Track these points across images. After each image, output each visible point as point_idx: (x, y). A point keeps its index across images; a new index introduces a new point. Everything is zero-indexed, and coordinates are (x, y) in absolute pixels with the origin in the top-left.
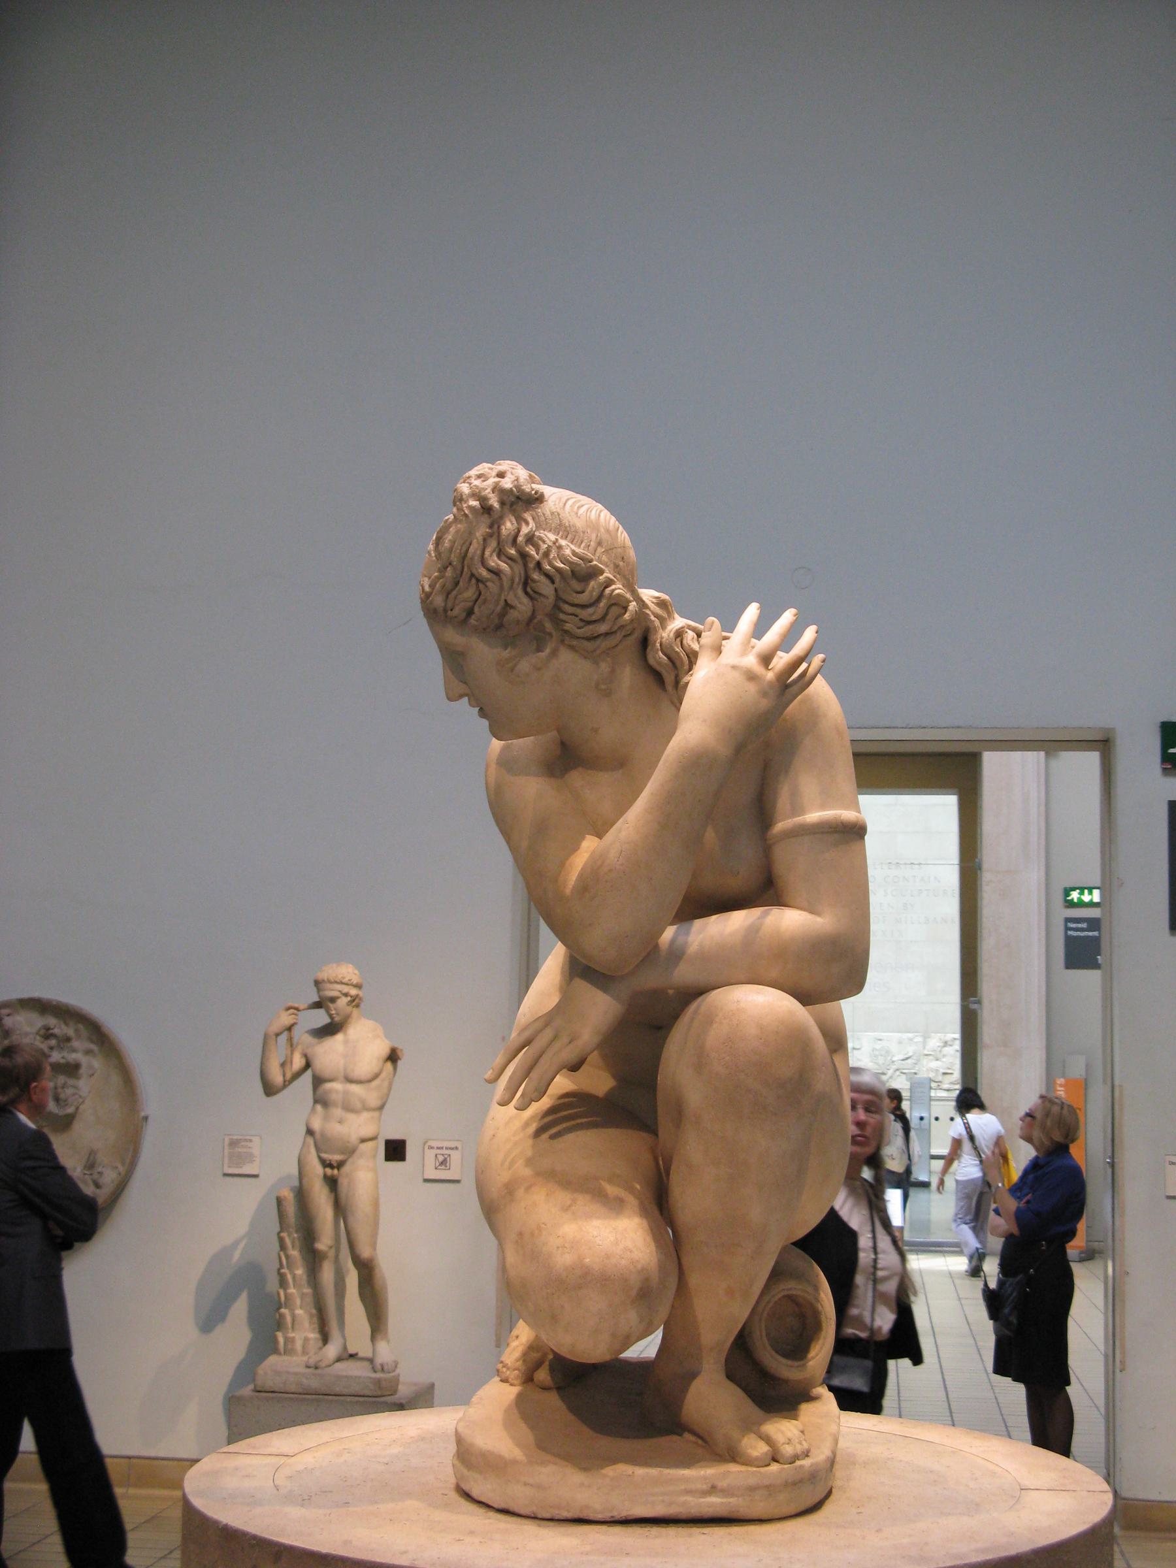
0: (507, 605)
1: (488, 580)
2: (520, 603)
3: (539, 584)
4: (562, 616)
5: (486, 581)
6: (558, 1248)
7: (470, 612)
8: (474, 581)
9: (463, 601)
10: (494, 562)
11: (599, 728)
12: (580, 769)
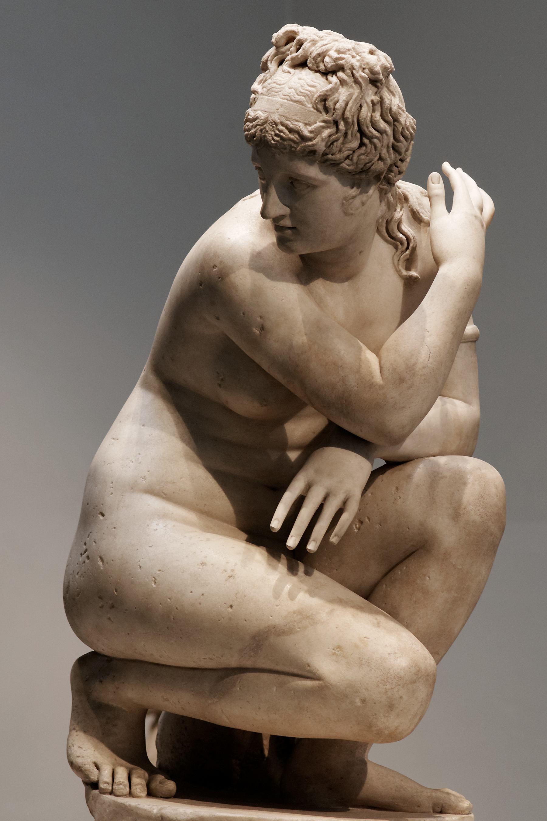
0: (381, 159)
1: (377, 138)
3: (401, 144)
4: (395, 169)
5: (372, 138)
6: (389, 654)
7: (347, 157)
8: (358, 135)
9: (348, 150)
10: (382, 125)
11: (363, 251)
12: (321, 279)
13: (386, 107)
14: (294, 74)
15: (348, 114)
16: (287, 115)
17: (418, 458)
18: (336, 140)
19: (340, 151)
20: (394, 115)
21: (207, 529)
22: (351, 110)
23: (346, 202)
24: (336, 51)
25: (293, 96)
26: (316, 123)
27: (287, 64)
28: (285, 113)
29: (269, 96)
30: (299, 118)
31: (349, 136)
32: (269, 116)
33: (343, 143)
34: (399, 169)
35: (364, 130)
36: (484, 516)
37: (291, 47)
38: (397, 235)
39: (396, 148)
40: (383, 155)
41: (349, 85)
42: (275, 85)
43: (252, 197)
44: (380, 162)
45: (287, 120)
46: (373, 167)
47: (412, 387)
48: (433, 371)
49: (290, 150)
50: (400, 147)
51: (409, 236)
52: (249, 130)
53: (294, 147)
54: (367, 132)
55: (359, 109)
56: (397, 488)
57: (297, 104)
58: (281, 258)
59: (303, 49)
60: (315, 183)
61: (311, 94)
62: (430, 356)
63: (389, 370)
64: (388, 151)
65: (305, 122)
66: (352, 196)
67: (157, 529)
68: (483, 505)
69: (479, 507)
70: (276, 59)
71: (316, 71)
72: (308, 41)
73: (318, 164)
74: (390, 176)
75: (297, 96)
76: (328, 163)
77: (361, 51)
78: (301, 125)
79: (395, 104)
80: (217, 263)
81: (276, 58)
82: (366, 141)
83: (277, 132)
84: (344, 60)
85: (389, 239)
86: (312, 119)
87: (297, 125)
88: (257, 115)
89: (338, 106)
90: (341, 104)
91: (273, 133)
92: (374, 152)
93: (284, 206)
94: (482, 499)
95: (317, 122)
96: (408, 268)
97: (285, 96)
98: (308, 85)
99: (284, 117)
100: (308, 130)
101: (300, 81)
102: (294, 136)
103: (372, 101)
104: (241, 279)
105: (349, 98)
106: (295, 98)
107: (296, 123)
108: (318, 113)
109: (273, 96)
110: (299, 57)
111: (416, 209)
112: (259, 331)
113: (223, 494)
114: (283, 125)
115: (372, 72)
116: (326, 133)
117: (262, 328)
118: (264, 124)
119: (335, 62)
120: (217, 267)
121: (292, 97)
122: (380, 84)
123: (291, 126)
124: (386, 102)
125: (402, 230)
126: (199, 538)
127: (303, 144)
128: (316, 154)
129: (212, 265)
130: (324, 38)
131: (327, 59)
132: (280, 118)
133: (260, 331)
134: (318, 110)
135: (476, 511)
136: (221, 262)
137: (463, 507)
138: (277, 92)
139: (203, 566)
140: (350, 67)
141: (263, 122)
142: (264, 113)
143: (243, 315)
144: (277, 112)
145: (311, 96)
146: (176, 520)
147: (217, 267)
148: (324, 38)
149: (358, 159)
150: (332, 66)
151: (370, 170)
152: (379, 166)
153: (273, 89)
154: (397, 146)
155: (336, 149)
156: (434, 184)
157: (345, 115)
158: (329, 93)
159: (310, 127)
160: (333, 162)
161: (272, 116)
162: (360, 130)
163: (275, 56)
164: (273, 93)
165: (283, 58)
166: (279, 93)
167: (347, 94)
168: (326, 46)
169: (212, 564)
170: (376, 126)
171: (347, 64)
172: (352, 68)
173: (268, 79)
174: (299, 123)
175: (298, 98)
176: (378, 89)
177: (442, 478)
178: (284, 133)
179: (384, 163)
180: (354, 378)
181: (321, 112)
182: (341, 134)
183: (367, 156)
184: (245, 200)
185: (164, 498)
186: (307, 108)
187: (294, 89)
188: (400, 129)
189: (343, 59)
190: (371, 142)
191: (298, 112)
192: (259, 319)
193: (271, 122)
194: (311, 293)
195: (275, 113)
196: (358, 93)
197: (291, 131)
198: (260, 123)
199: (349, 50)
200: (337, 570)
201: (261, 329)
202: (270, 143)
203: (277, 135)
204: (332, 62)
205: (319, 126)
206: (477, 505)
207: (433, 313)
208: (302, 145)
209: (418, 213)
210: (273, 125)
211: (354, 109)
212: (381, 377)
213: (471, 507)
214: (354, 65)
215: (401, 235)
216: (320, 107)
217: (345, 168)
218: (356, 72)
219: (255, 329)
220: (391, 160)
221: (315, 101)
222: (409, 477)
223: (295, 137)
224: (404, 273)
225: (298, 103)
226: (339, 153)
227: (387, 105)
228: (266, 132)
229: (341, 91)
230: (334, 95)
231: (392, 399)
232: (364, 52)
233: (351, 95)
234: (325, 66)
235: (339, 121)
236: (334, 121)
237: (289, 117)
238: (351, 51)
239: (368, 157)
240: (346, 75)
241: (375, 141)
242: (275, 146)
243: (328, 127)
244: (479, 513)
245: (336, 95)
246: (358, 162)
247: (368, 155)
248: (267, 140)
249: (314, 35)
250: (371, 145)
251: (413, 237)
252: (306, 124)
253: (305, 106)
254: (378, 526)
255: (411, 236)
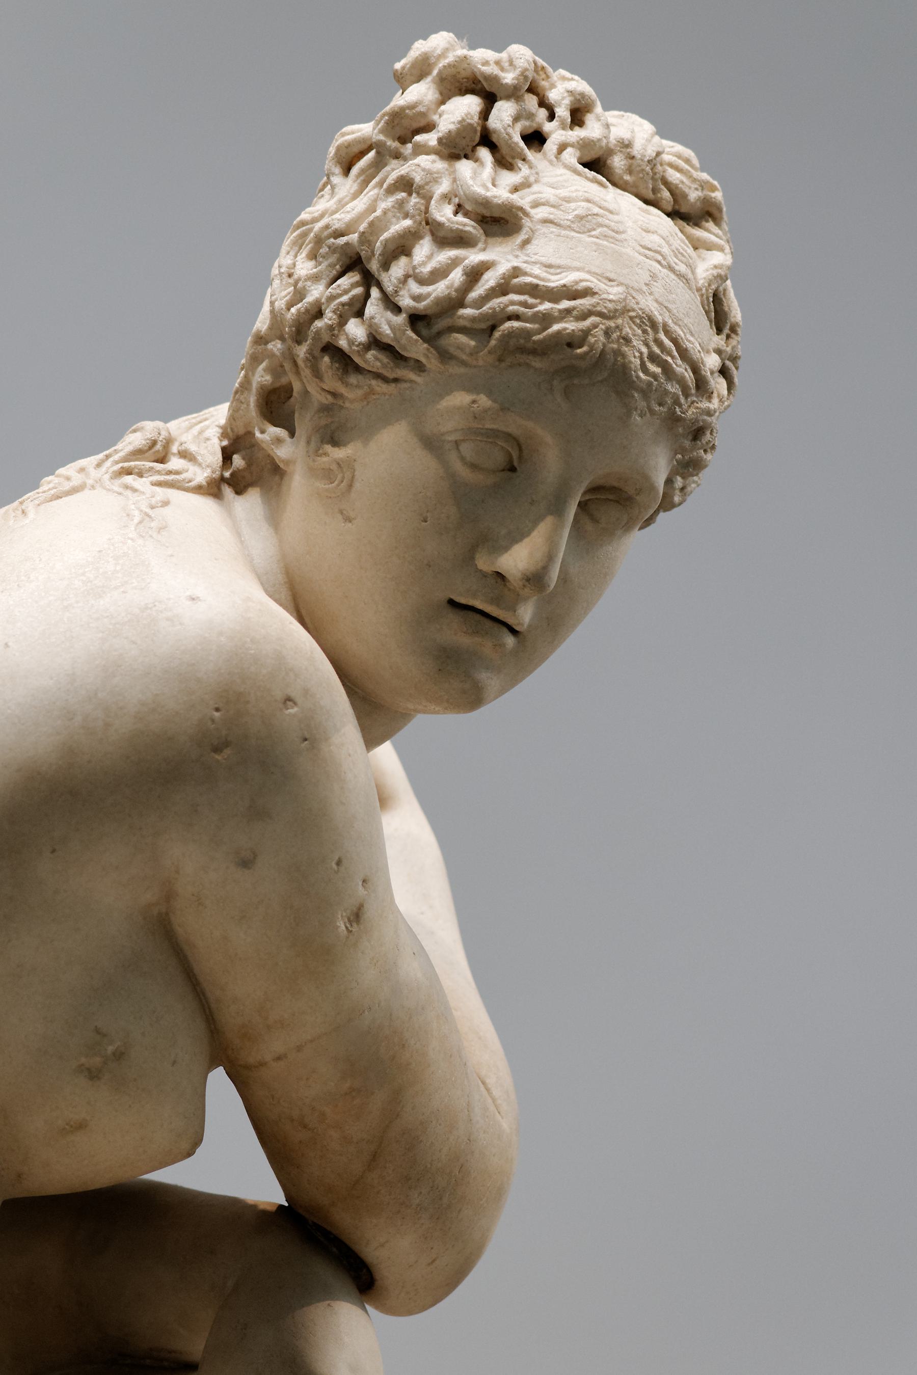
52: (546, 319)
83: (656, 350)
97: (649, 249)
114: (667, 332)
117: (357, 916)
129: (279, 695)
136: (306, 692)
147: (295, 704)
193: (641, 318)
201: (352, 918)
203: (653, 358)
242: (646, 392)
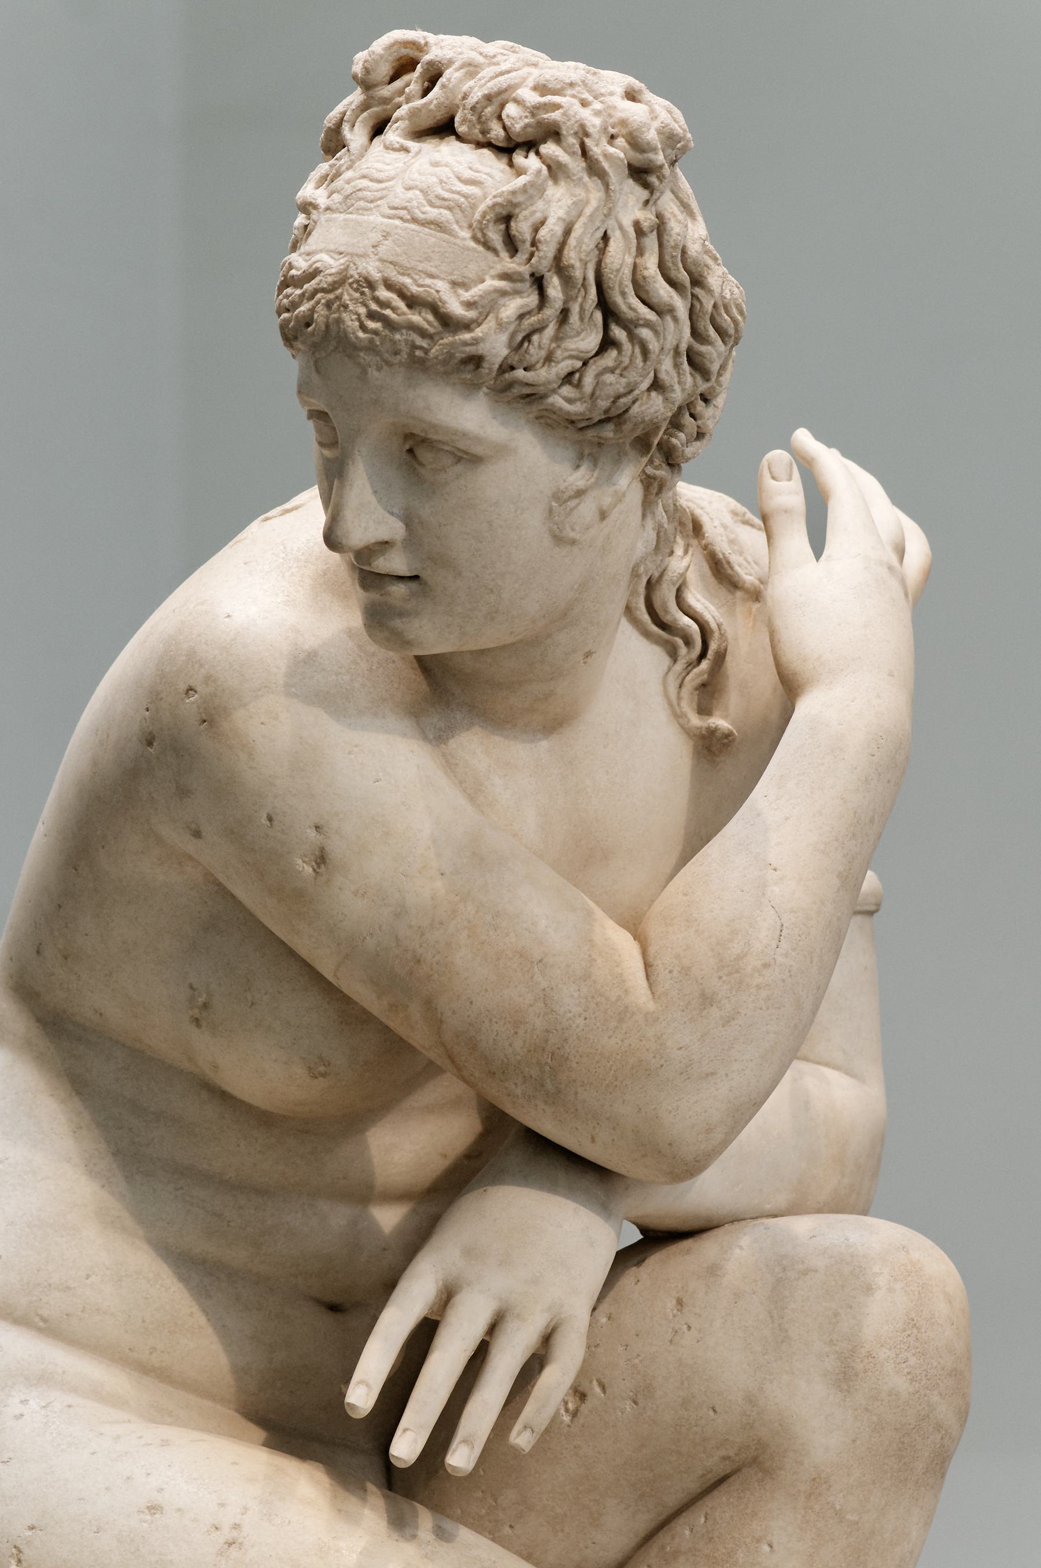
0: (657, 385)
1: (648, 324)
2: (679, 383)
3: (709, 348)
4: (687, 420)
7: (568, 378)
8: (598, 316)
9: (571, 357)
13: (672, 244)
14: (418, 153)
15: (571, 256)
16: (403, 260)
17: (732, 1222)
18: (539, 330)
19: (549, 359)
20: (693, 268)
21: (157, 1415)
22: (581, 248)
23: (560, 506)
24: (535, 88)
25: (418, 207)
26: (483, 281)
27: (397, 129)
28: (397, 255)
29: (351, 213)
30: (436, 267)
31: (574, 318)
32: (352, 265)
33: (557, 338)
34: (699, 422)
35: (615, 303)
36: (919, 1377)
37: (408, 85)
38: (675, 620)
39: (698, 359)
40: (663, 376)
41: (575, 178)
42: (364, 183)
43: (288, 511)
44: (654, 394)
45: (403, 274)
46: (635, 409)
47: (734, 1019)
48: (791, 976)
49: (411, 355)
50: (708, 357)
51: (707, 623)
53: (421, 348)
54: (623, 308)
55: (601, 245)
56: (680, 1302)
57: (431, 229)
58: (370, 670)
59: (443, 86)
60: (478, 450)
61: (469, 202)
62: (781, 936)
63: (671, 972)
64: (677, 366)
65: (454, 278)
66: (575, 488)
67: (22, 1415)
68: (917, 1348)
69: (906, 1354)
70: (365, 119)
71: (479, 145)
72: (457, 65)
73: (486, 394)
74: (674, 441)
75: (428, 208)
76: (516, 391)
77: (603, 91)
78: (442, 285)
79: (696, 236)
80: (196, 682)
81: (365, 114)
82: (618, 333)
83: (374, 307)
84: (561, 111)
85: (655, 629)
86: (471, 271)
87: (429, 286)
88: (318, 265)
89: (543, 233)
90: (552, 227)
91: (362, 310)
92: (641, 364)
93: (387, 515)
94: (915, 1331)
95: (487, 277)
96: (704, 710)
97: (396, 208)
98: (459, 178)
99: (392, 267)
100: (461, 299)
101: (438, 169)
102: (422, 317)
103: (637, 225)
104: (262, 723)
105: (574, 213)
106: (423, 213)
107: (428, 281)
108: (490, 255)
109: (361, 212)
110: (432, 107)
111: (724, 554)
112: (312, 867)
113: (201, 1319)
114: (389, 286)
115: (635, 143)
116: (511, 308)
117: (321, 859)
118: (336, 286)
119: (533, 115)
120: (196, 692)
121: (417, 211)
122: (658, 177)
123: (415, 289)
124: (672, 229)
125: (690, 606)
126: (141, 1437)
127: (448, 339)
128: (483, 367)
129: (183, 687)
130: (499, 58)
131: (511, 110)
132: (382, 269)
133: (315, 867)
134: (487, 245)
135: (898, 1364)
136: (208, 679)
137: (864, 1351)
138: (372, 202)
139: (154, 1514)
140: (576, 128)
141: (335, 282)
142: (336, 256)
143: (268, 823)
144: (372, 252)
145: (468, 209)
146: (74, 1390)
147: (196, 692)
148: (499, 58)
149: (598, 383)
150: (527, 126)
151: (627, 416)
152: (652, 406)
153: (360, 194)
154: (700, 354)
155: (537, 354)
156: (777, 480)
157: (564, 259)
158: (520, 198)
159: (467, 291)
160: (527, 391)
161: (358, 262)
162: (605, 305)
163: (363, 111)
164: (362, 203)
165: (384, 116)
166: (379, 202)
167: (570, 202)
168: (506, 76)
169: (179, 1510)
170: (647, 292)
171: (568, 121)
172: (583, 133)
173: (344, 172)
174: (435, 281)
175: (433, 213)
176: (652, 193)
177: (806, 1272)
178: (394, 309)
179: (666, 399)
180: (576, 995)
181: (495, 251)
182: (553, 310)
183: (621, 375)
184: (267, 519)
185: (40, 1330)
186: (458, 241)
187: (421, 191)
188: (709, 307)
189: (557, 107)
190: (632, 337)
191: (433, 252)
192: (312, 834)
193: (357, 282)
194: (450, 765)
195: (368, 256)
196: (600, 200)
197: (413, 302)
198: (325, 286)
199: (572, 85)
200: (511, 1526)
201: (318, 861)
202: (353, 339)
203: (372, 315)
204: (526, 117)
205: (492, 288)
206: (902, 1346)
207: (787, 819)
208: (445, 341)
209: (729, 563)
210: (364, 289)
211: (590, 242)
212: (649, 992)
213: (887, 1351)
214: (588, 124)
215: (686, 621)
216: (495, 236)
217: (561, 409)
218: (594, 143)
219: (299, 862)
220: (683, 390)
221: (480, 222)
222: (713, 1271)
223: (425, 319)
224: (696, 721)
225: (432, 227)
226: (547, 365)
227: (675, 237)
228: (342, 309)
229: (553, 195)
230: (532, 205)
231: (680, 1053)
232: (611, 94)
233: (579, 207)
234: (504, 128)
235: (547, 275)
236: (532, 275)
237: (408, 265)
238: (578, 89)
239: (624, 377)
240: (565, 151)
241: (645, 333)
242: (371, 348)
243: (517, 293)
244: (906, 1370)
245: (540, 205)
246: (598, 393)
247: (625, 373)
248: (345, 331)
249: (472, 50)
250: (633, 345)
251: (719, 626)
252: (454, 284)
253: (453, 236)
254: (628, 1405)
255: (714, 621)
